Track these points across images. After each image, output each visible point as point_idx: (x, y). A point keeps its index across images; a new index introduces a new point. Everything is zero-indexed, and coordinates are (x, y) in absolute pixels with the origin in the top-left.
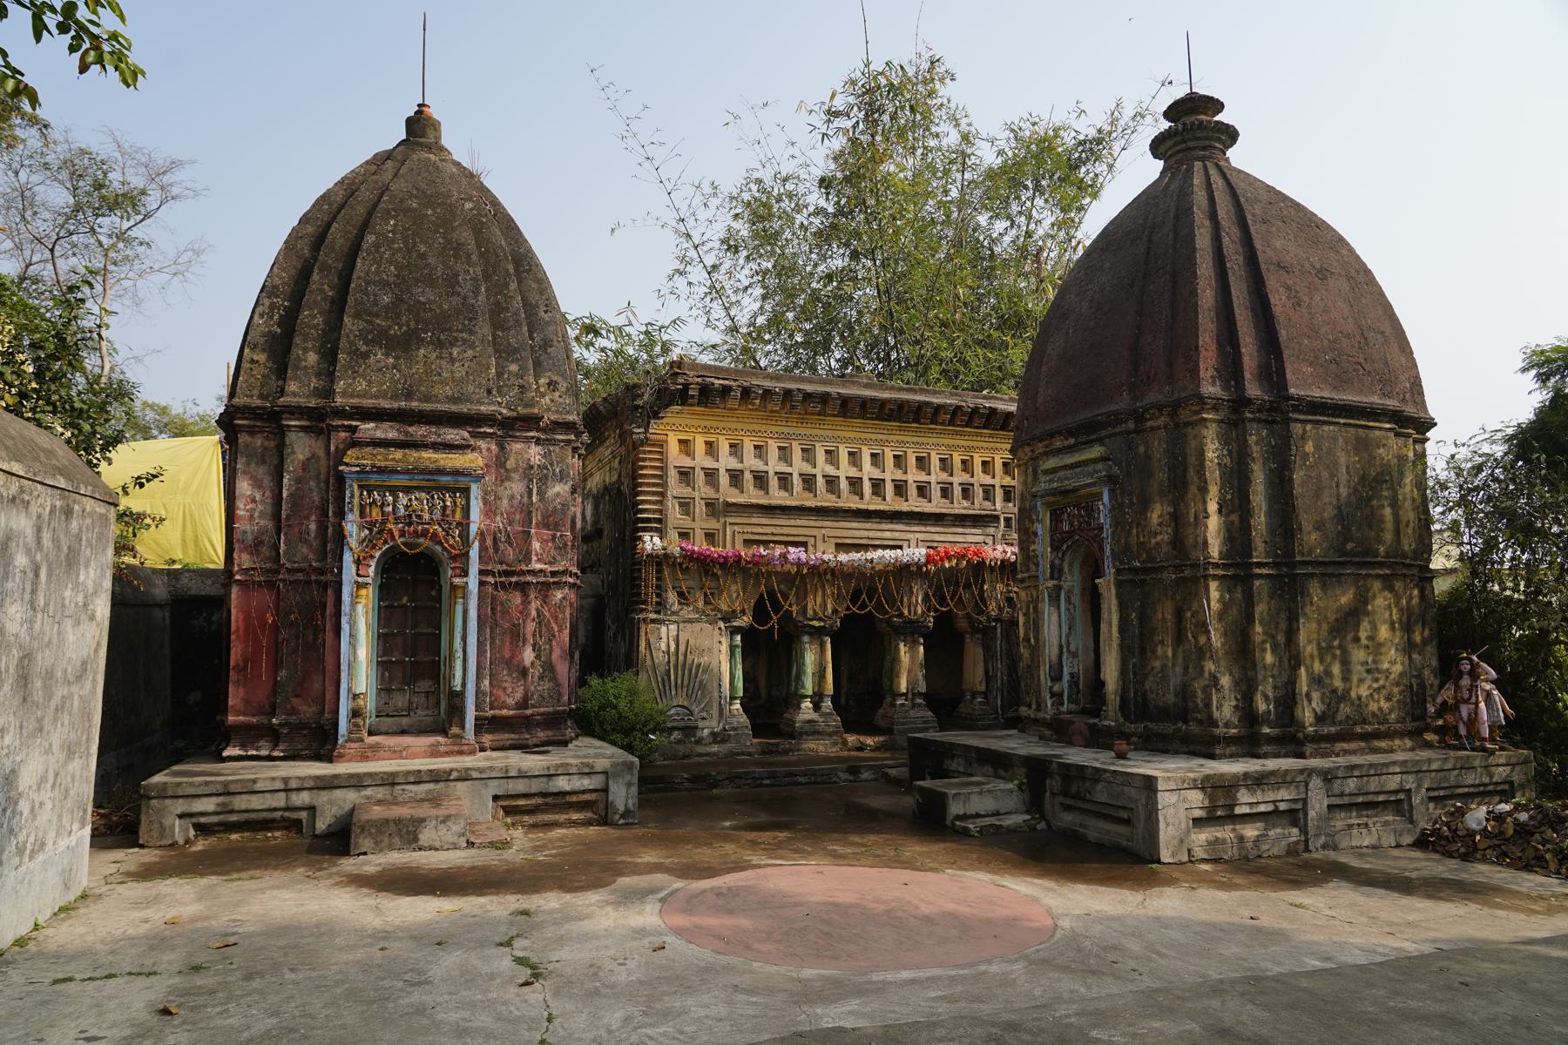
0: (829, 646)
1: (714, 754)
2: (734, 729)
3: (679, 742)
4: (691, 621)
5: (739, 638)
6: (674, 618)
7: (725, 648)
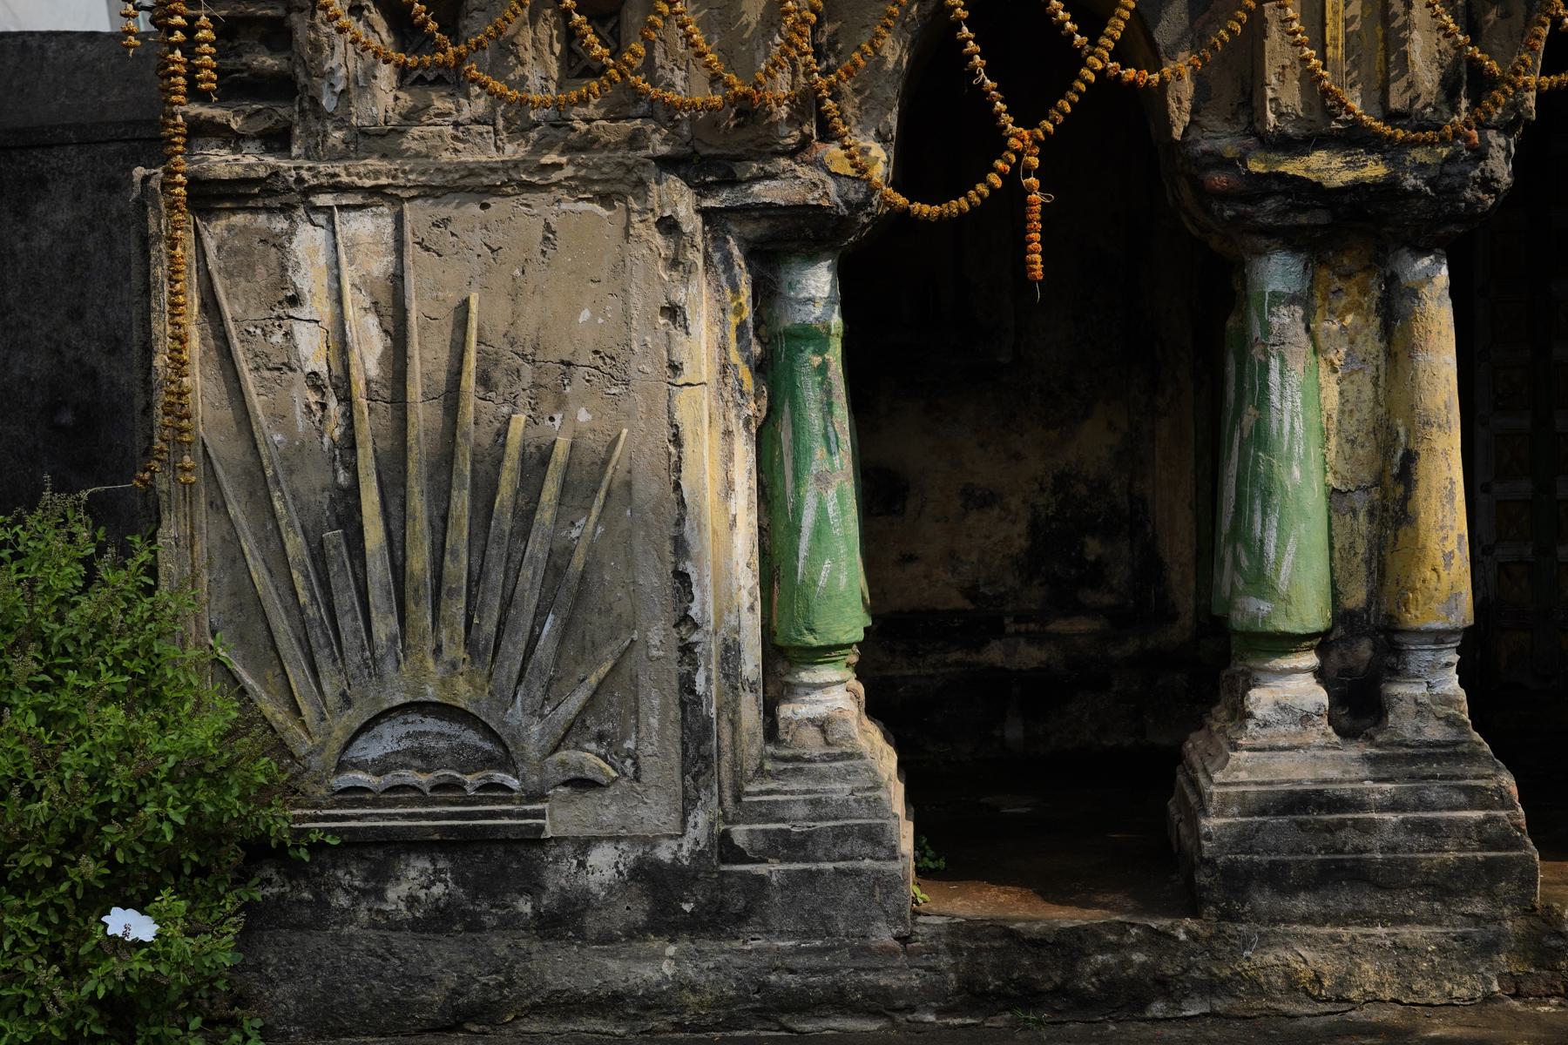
0: (1437, 318)
1: (651, 1002)
2: (789, 845)
3: (438, 920)
4: (475, 186)
5: (817, 284)
6: (370, 169)
7: (707, 337)
